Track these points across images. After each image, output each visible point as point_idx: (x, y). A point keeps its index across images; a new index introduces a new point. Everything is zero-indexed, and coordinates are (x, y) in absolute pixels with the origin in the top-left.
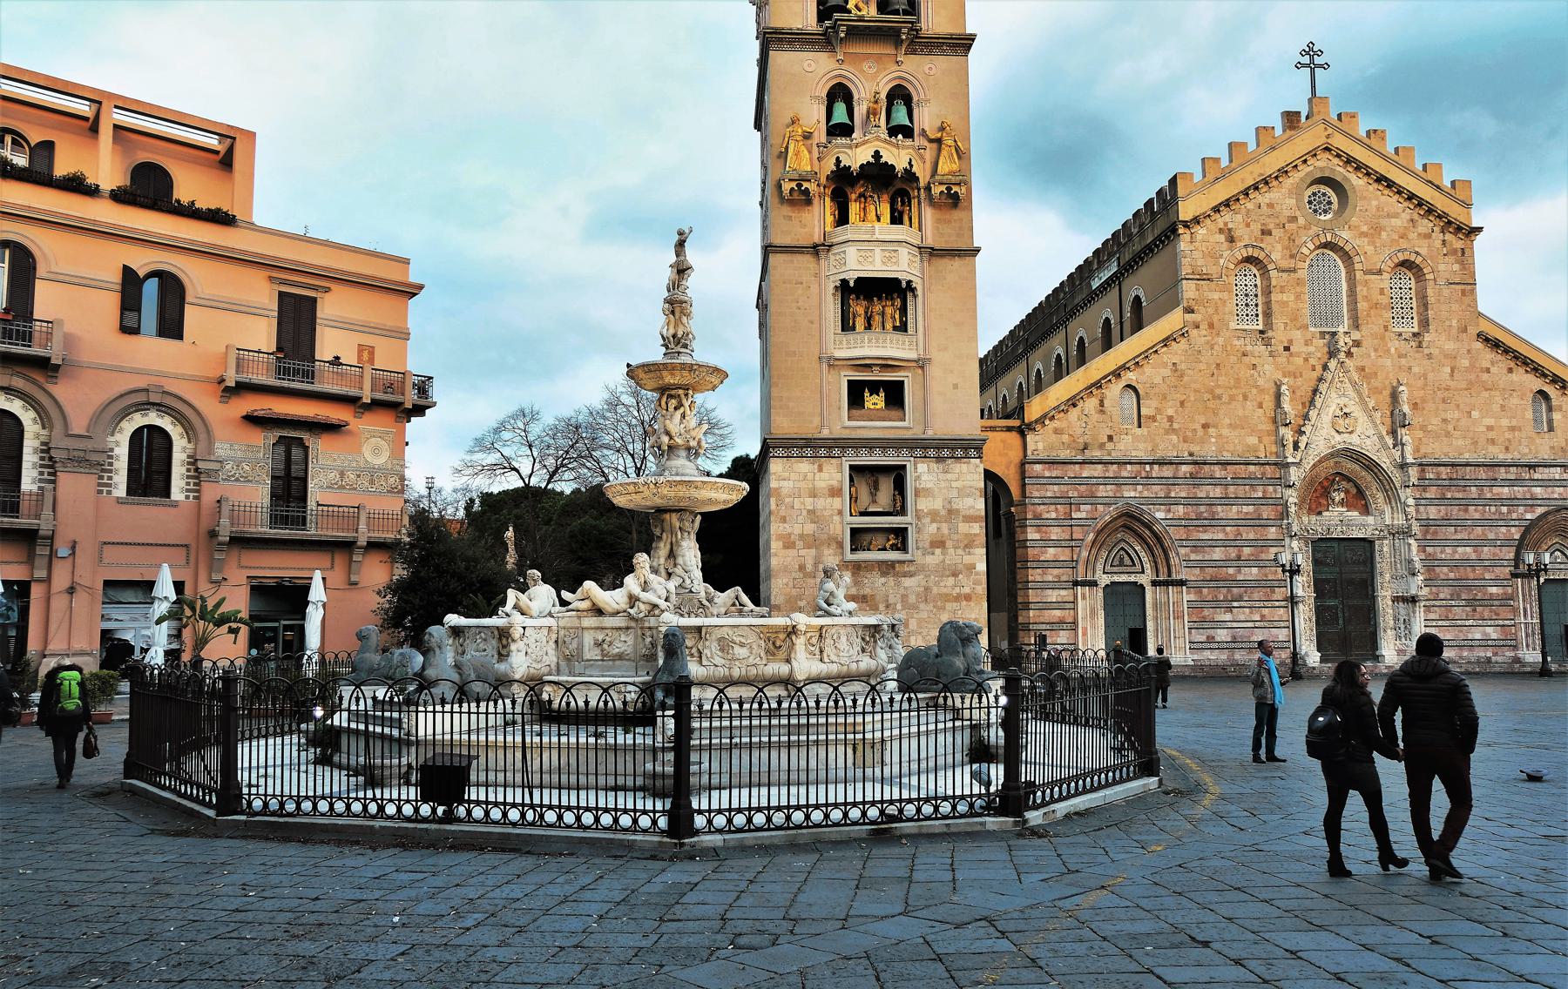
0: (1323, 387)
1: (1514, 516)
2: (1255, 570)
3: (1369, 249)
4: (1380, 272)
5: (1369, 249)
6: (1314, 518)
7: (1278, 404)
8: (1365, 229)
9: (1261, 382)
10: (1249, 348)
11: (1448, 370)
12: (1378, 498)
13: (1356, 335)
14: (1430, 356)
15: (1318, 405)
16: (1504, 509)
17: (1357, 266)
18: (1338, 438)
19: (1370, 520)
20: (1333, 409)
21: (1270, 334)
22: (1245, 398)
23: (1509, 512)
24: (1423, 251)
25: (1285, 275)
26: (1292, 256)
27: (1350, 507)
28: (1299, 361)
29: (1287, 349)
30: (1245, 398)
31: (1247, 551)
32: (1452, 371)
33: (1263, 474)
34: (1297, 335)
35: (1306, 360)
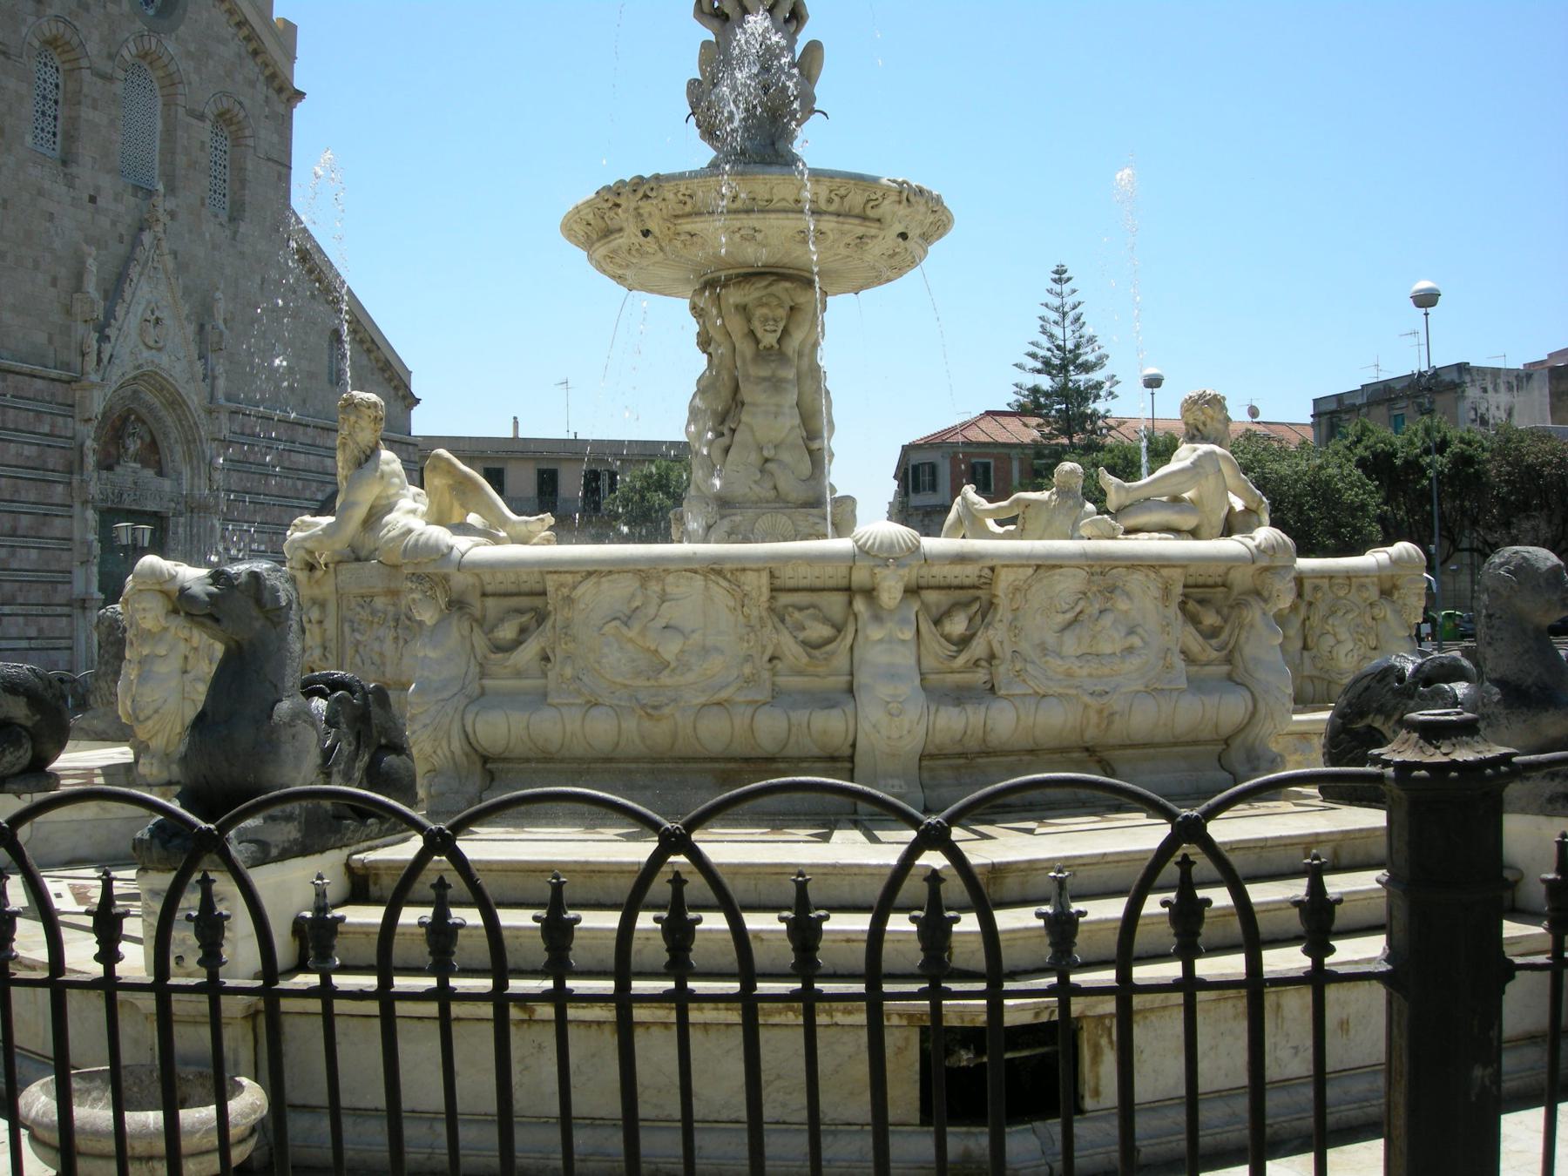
0: (134, 271)
1: (308, 495)
2: (34, 554)
3: (194, 78)
4: (201, 117)
5: (194, 78)
6: (104, 474)
7: (78, 287)
8: (192, 47)
9: (57, 244)
10: (47, 185)
11: (258, 279)
12: (176, 455)
13: (170, 204)
14: (242, 254)
15: (128, 296)
16: (300, 484)
17: (181, 100)
18: (146, 354)
19: (167, 484)
20: (139, 310)
21: (74, 170)
22: (36, 266)
23: (304, 488)
24: (247, 103)
25: (100, 82)
26: (111, 57)
27: (145, 464)
28: (105, 222)
29: (93, 199)
30: (36, 266)
31: (25, 521)
32: (263, 280)
33: (53, 395)
34: (106, 182)
35: (114, 223)
